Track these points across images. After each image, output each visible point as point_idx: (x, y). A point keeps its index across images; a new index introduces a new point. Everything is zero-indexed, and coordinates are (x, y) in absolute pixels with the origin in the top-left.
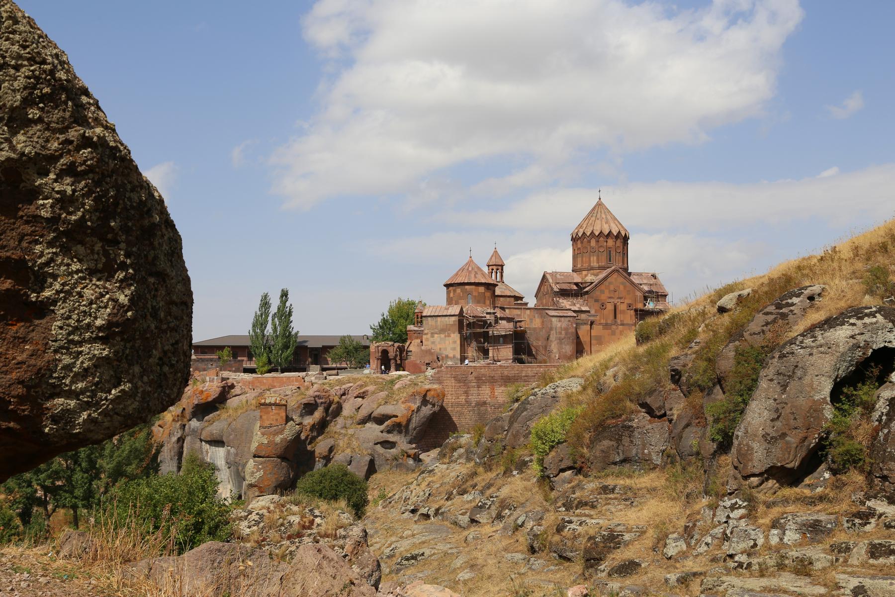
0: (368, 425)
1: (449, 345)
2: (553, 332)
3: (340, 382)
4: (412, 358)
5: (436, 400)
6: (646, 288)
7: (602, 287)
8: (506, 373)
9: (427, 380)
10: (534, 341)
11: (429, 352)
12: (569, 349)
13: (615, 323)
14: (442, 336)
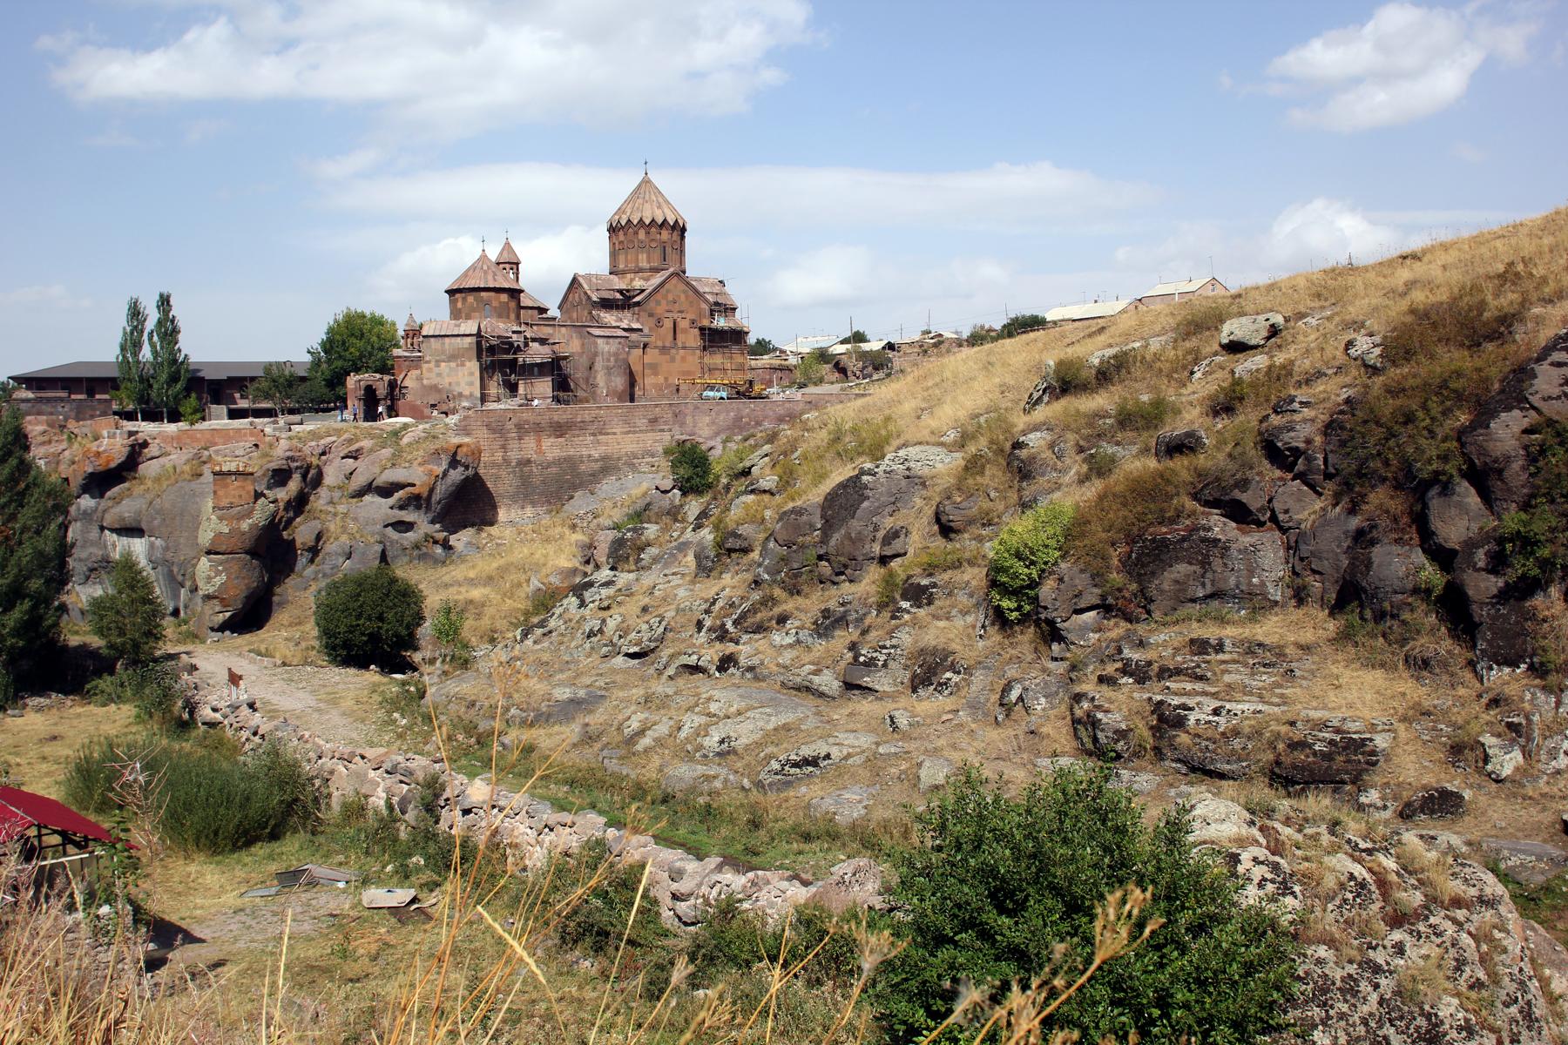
0: (367, 498)
1: (465, 377)
2: (599, 358)
3: (315, 435)
4: (409, 397)
5: (470, 460)
6: (711, 298)
7: (658, 296)
8: (556, 418)
9: (449, 430)
10: (576, 371)
11: (435, 388)
12: (620, 382)
13: (675, 346)
14: (453, 365)
